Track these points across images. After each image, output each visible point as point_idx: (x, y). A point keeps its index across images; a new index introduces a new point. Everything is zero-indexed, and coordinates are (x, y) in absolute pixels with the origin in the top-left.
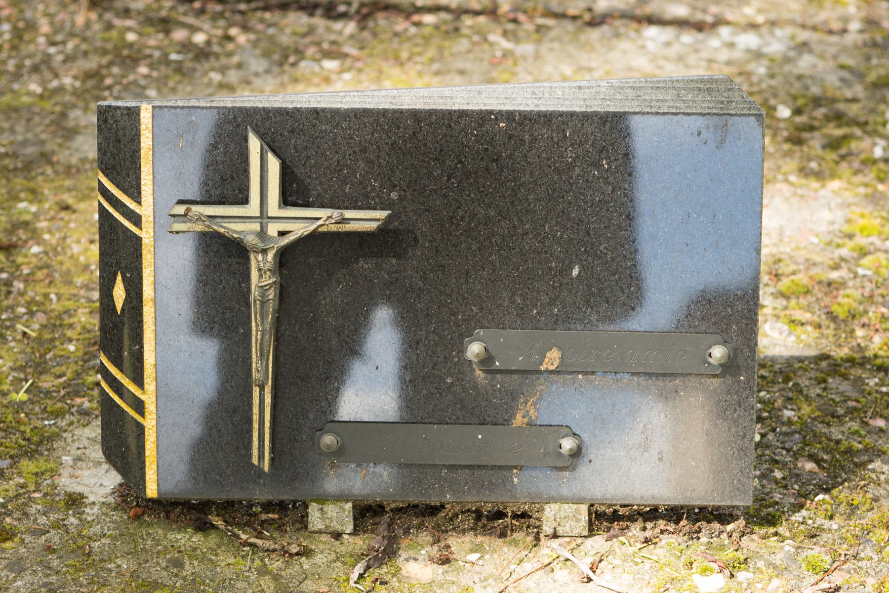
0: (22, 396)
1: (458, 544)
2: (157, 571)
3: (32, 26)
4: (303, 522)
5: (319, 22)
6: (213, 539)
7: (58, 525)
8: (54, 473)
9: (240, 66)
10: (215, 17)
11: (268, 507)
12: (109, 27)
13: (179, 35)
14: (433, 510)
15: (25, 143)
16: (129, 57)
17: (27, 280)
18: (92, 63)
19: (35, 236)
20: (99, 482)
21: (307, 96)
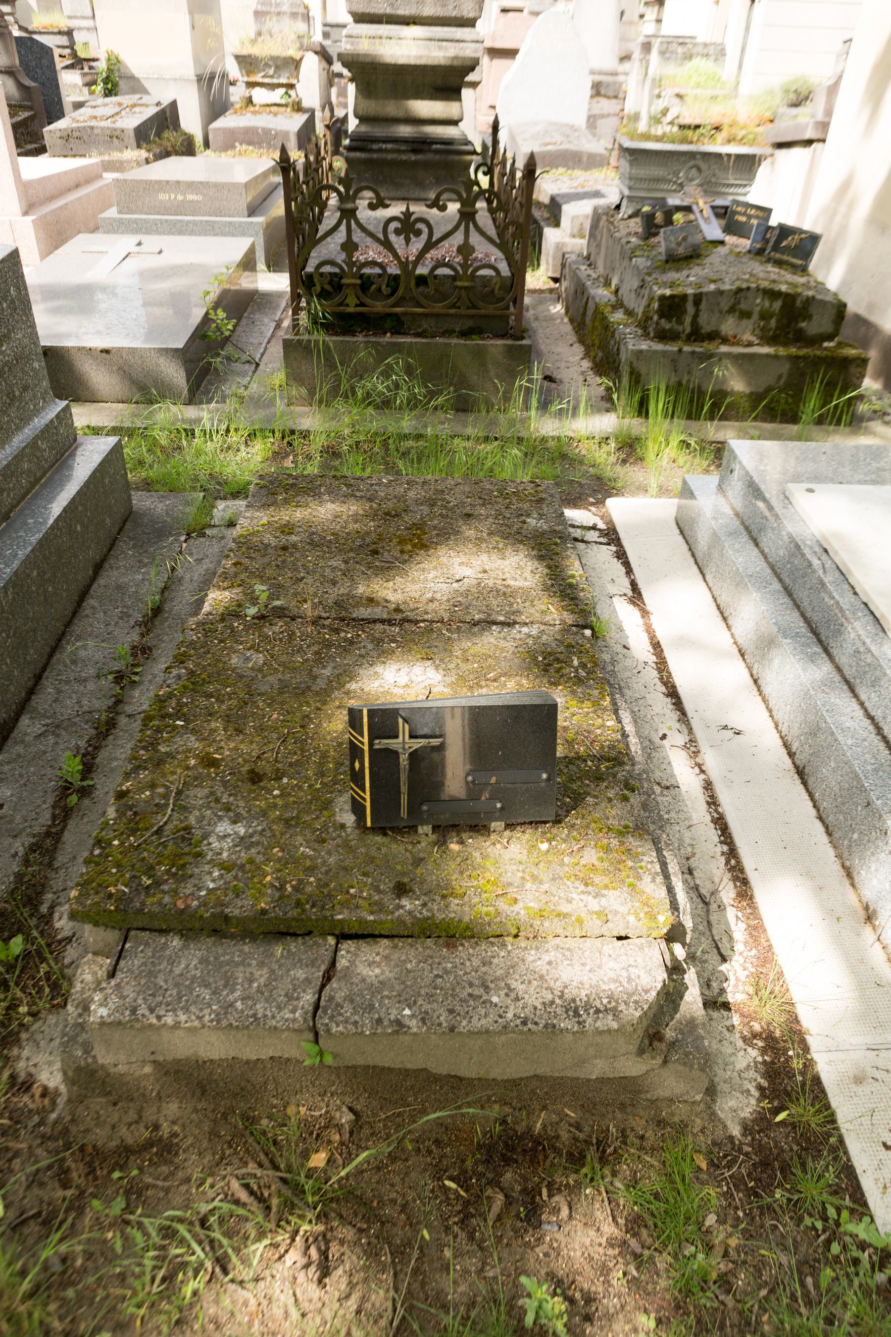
0: (318, 786)
1: (464, 836)
2: (373, 852)
3: (294, 633)
4: (416, 831)
5: (387, 627)
6: (389, 839)
7: (339, 836)
8: (334, 815)
9: (364, 647)
10: (353, 627)
11: (405, 827)
12: (319, 633)
13: (342, 635)
14: (454, 826)
15: (301, 683)
16: (329, 645)
17: (312, 739)
18: (315, 648)
19: (311, 720)
20: (349, 819)
21: (652, 1207)
